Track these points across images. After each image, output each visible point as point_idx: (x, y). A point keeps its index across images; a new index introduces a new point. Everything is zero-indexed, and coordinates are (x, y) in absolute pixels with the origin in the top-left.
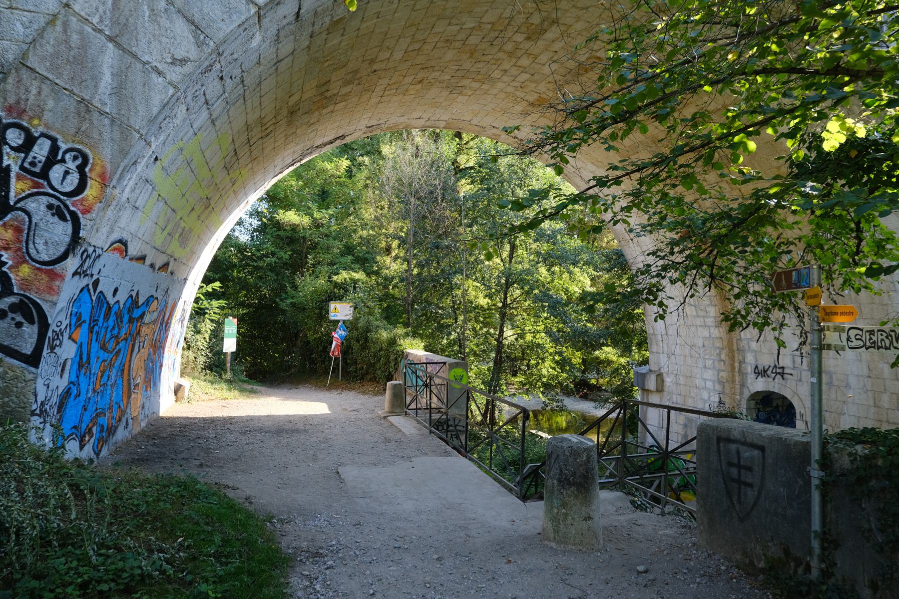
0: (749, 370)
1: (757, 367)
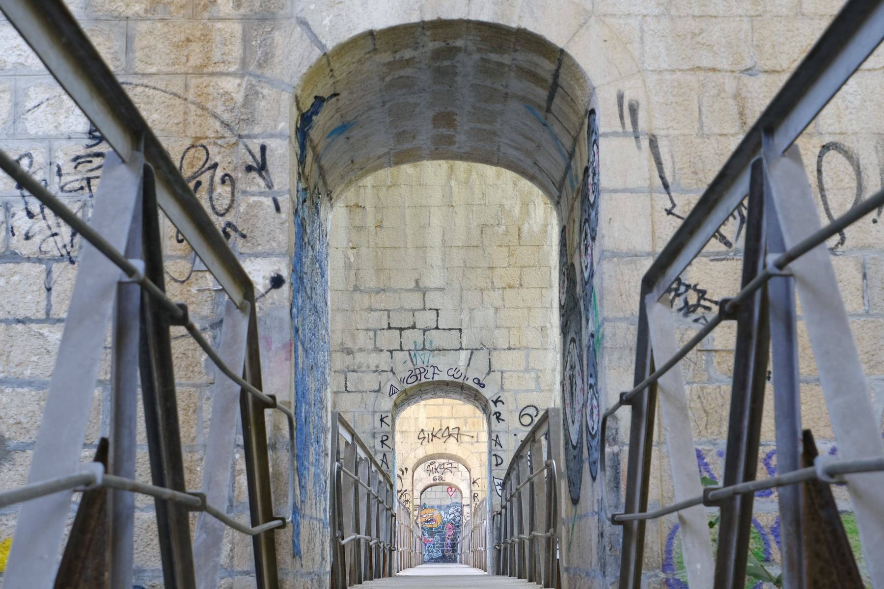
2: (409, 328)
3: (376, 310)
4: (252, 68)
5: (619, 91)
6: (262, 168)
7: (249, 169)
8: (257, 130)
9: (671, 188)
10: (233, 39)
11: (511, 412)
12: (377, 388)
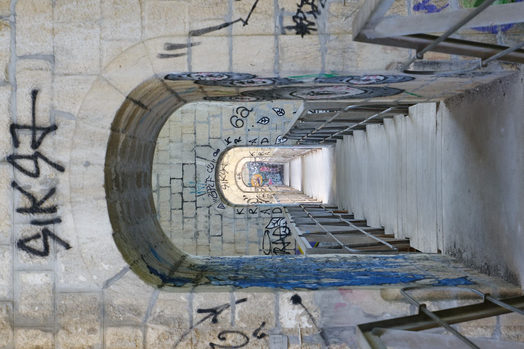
0: (37, 280)
1: (22, 244)
2: (182, 197)
3: (171, 217)
4: (140, 320)
5: (158, 57)
6: (214, 312)
7: (215, 321)
8: (186, 316)
9: (228, 21)
10: (119, 334)
11: (235, 133)
12: (220, 216)
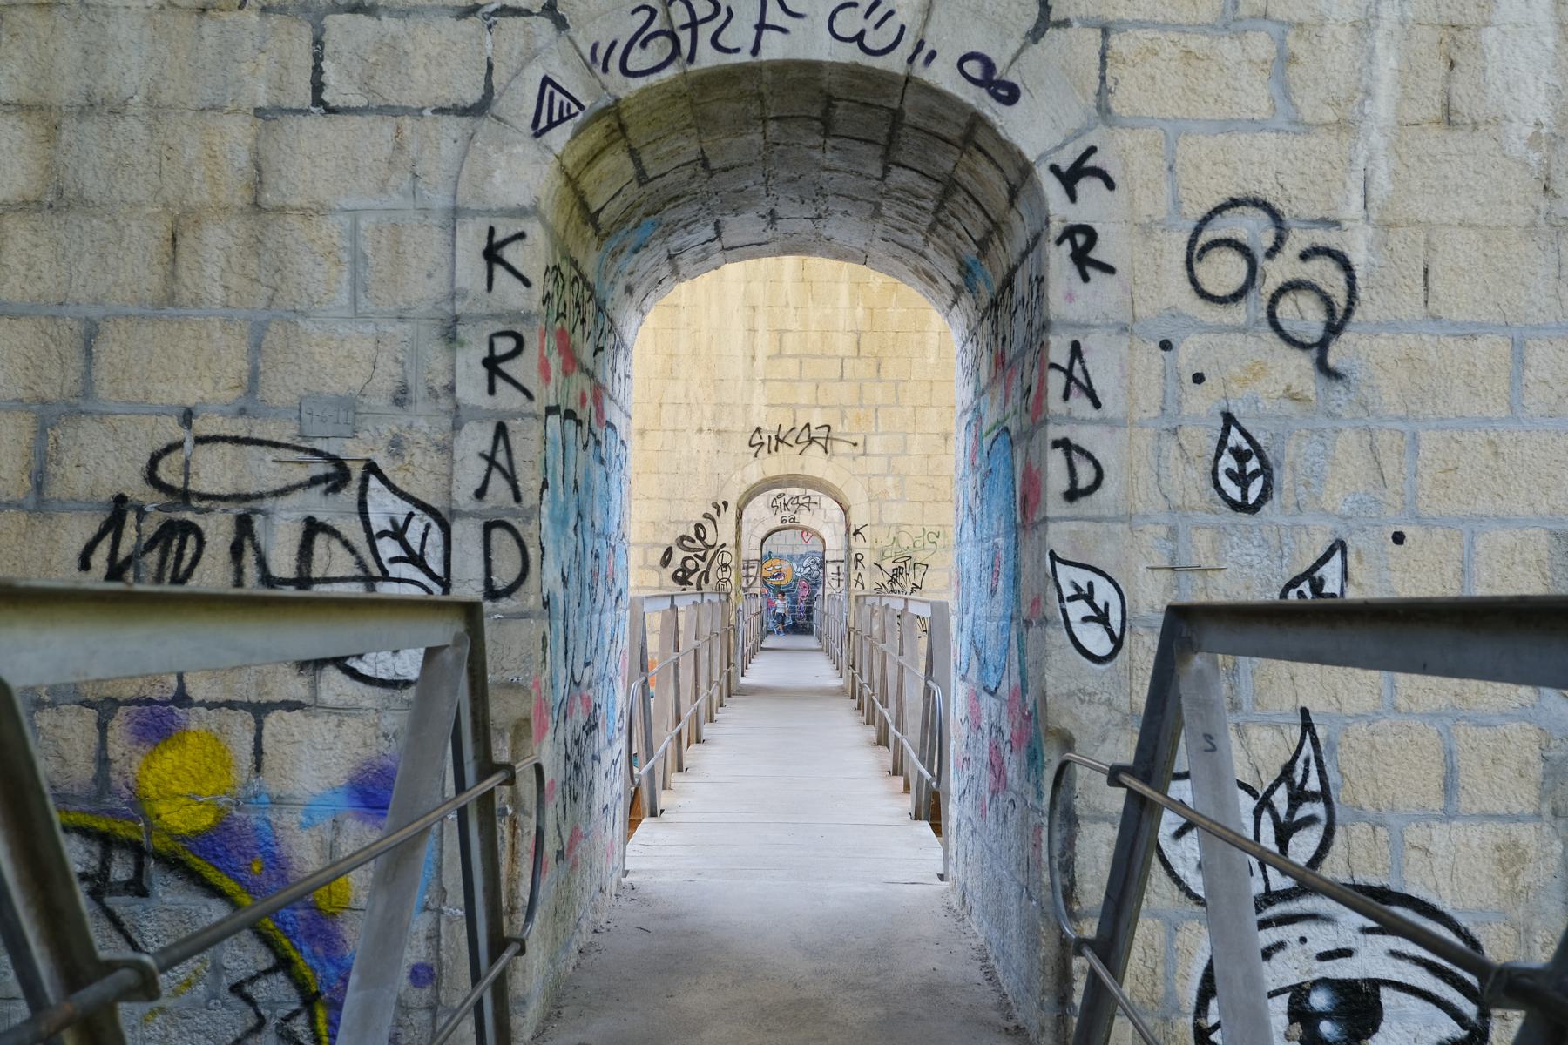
11: (1146, 230)
12: (473, 95)
